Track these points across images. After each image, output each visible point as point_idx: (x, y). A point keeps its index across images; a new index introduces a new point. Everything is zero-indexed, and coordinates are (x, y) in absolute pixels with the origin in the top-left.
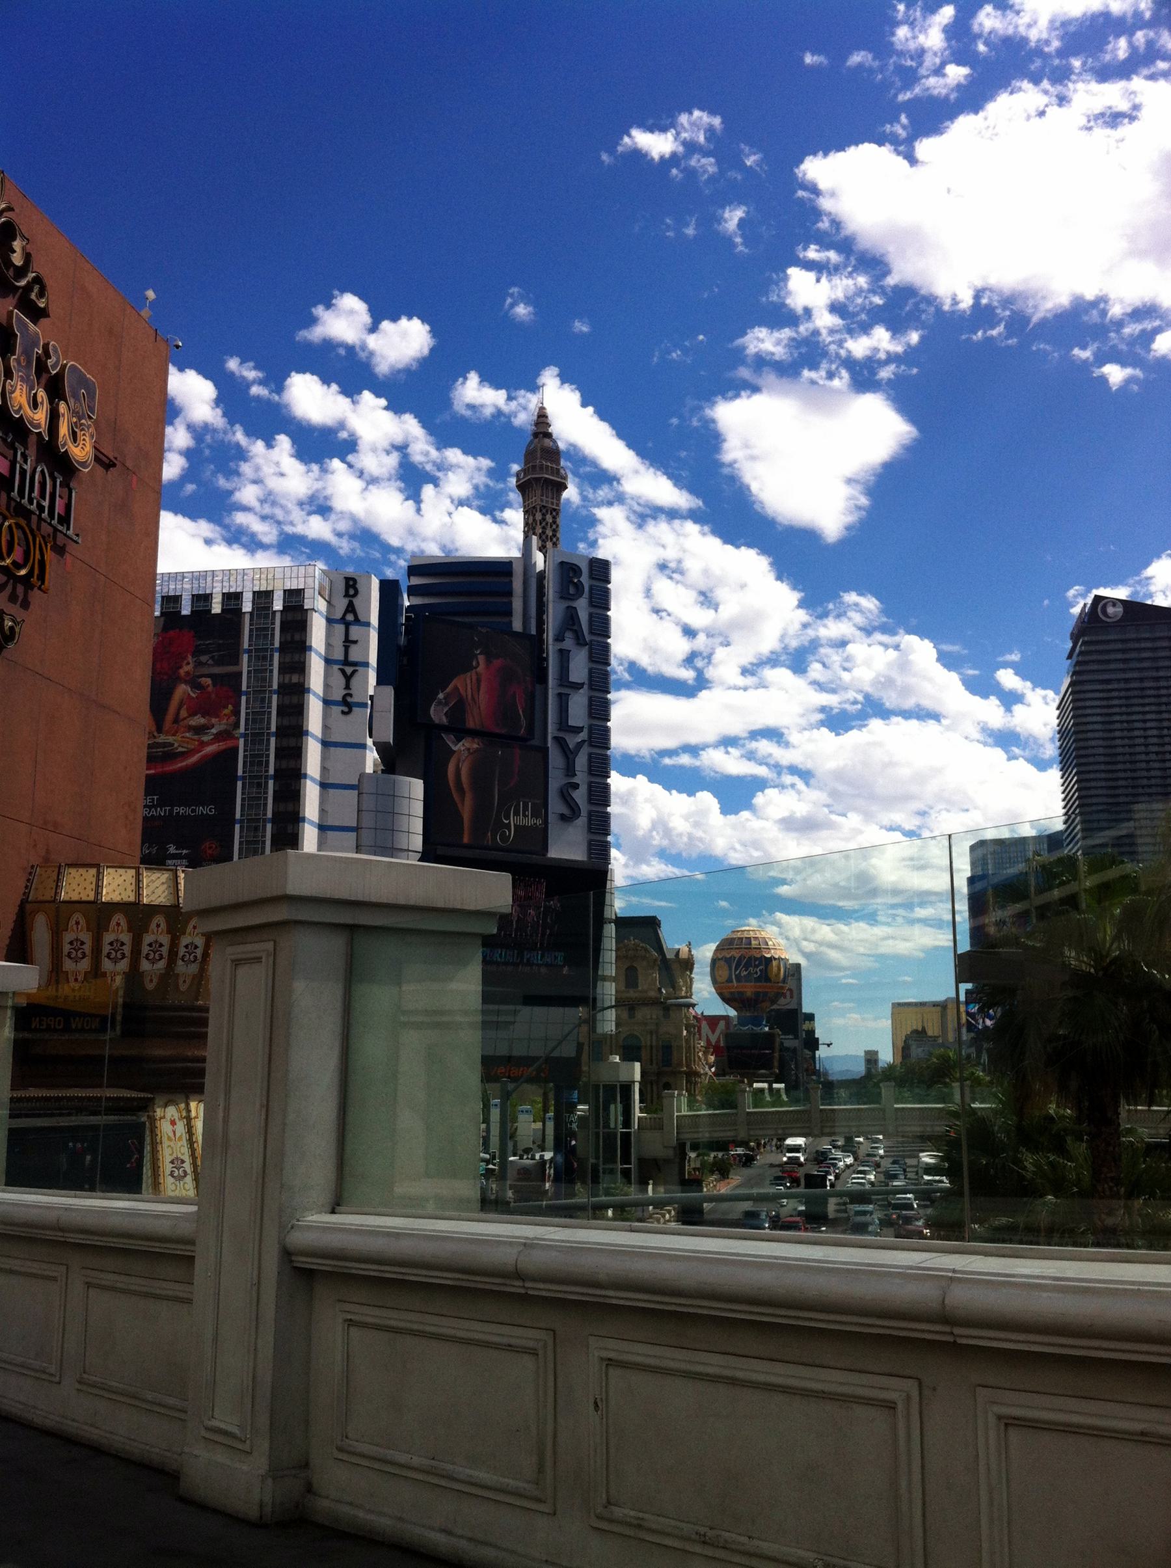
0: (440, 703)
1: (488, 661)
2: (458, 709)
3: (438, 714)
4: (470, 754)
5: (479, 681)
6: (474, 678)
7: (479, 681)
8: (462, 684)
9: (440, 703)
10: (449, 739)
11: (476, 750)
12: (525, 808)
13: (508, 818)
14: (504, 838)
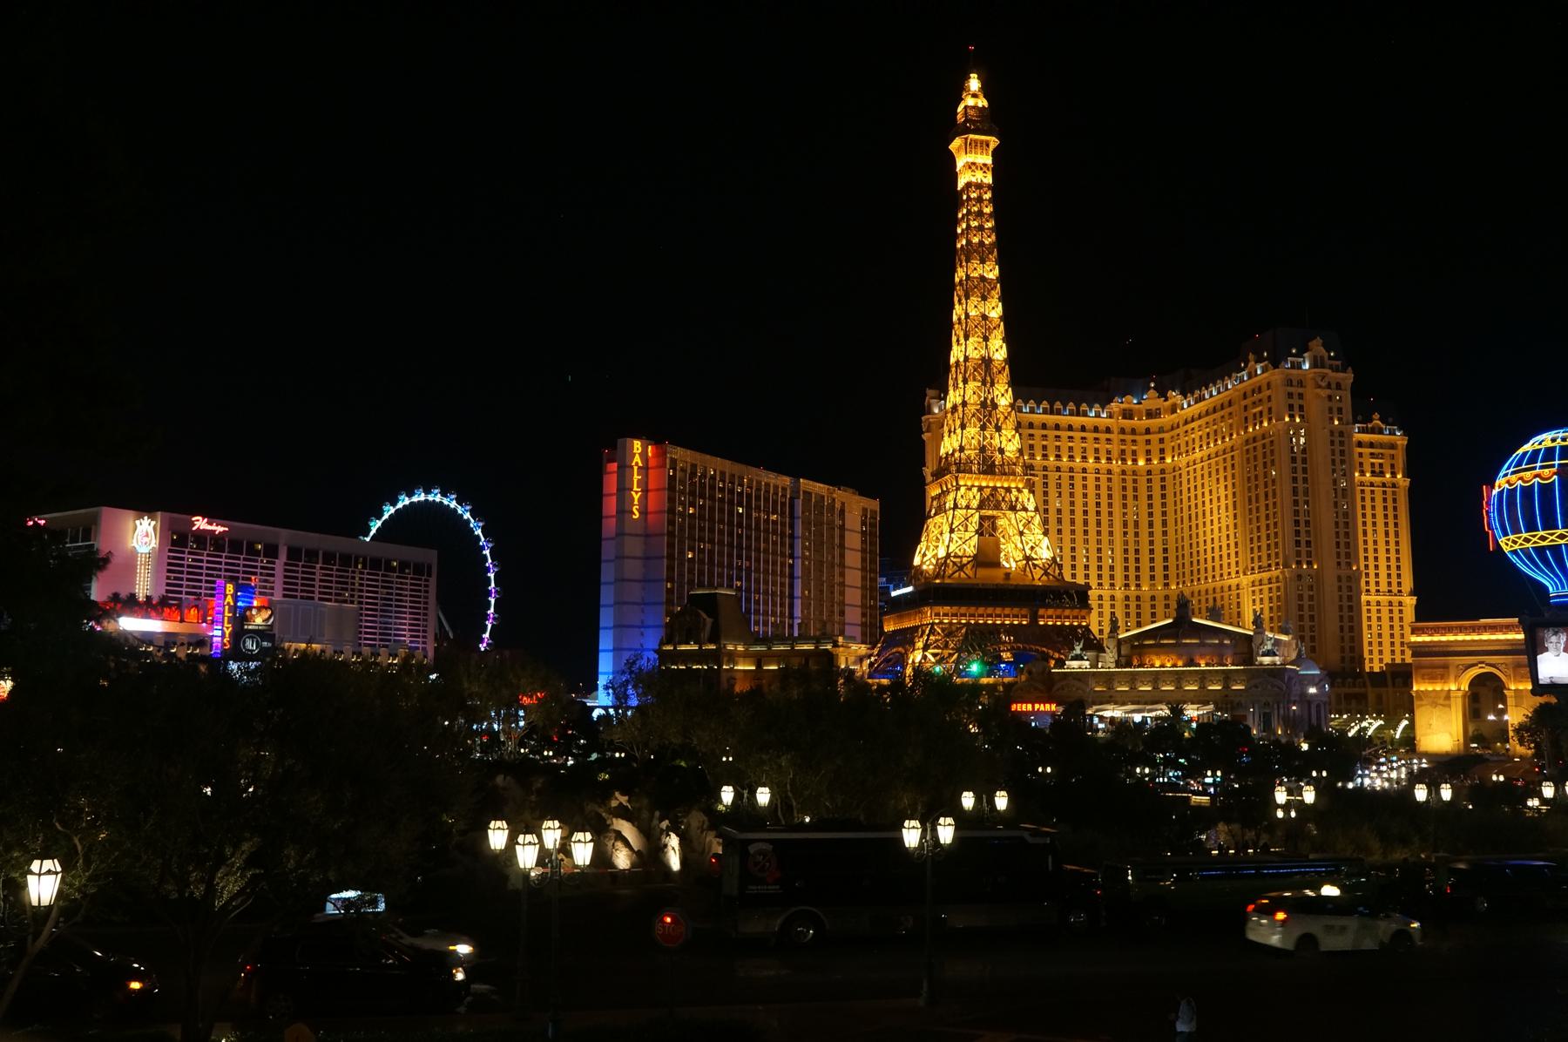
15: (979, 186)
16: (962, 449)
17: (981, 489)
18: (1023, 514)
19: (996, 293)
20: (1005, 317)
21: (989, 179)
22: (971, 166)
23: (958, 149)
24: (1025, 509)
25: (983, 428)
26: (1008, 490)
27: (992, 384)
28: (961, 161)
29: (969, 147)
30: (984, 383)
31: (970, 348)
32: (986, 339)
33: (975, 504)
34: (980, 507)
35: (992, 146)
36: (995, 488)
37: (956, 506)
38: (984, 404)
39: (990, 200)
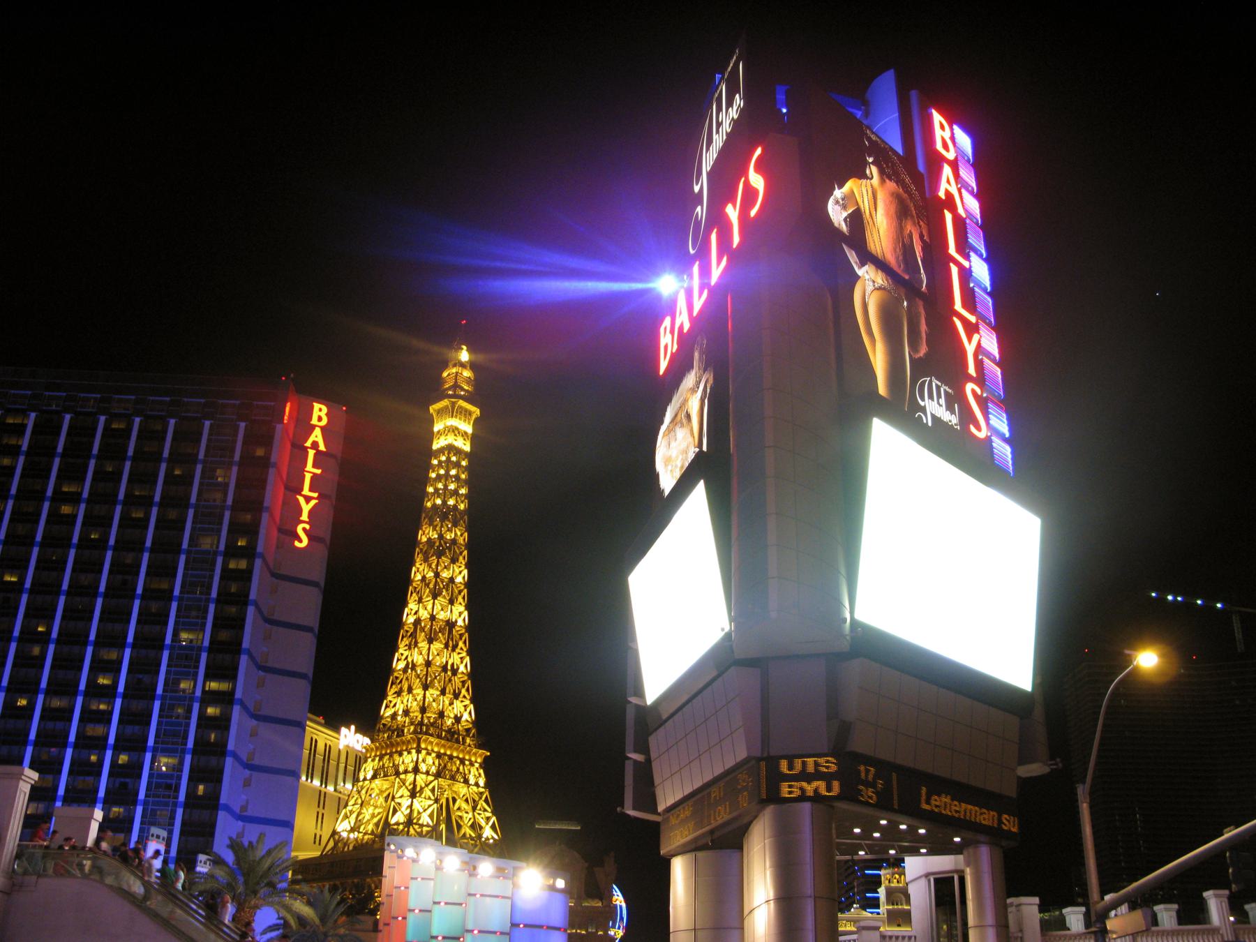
1: (882, 181)
2: (856, 219)
3: (837, 215)
10: (852, 257)
12: (939, 396)
13: (923, 400)
15: (458, 451)
16: (423, 710)
17: (439, 756)
18: (475, 788)
19: (462, 561)
20: (468, 585)
21: (467, 447)
22: (454, 430)
23: (439, 412)
24: (477, 785)
25: (443, 692)
26: (462, 761)
27: (453, 650)
28: (438, 427)
29: (452, 411)
30: (446, 646)
31: (438, 607)
32: (451, 602)
33: (433, 770)
34: (438, 775)
35: (474, 417)
36: (451, 757)
37: (416, 770)
38: (444, 668)
39: (466, 468)
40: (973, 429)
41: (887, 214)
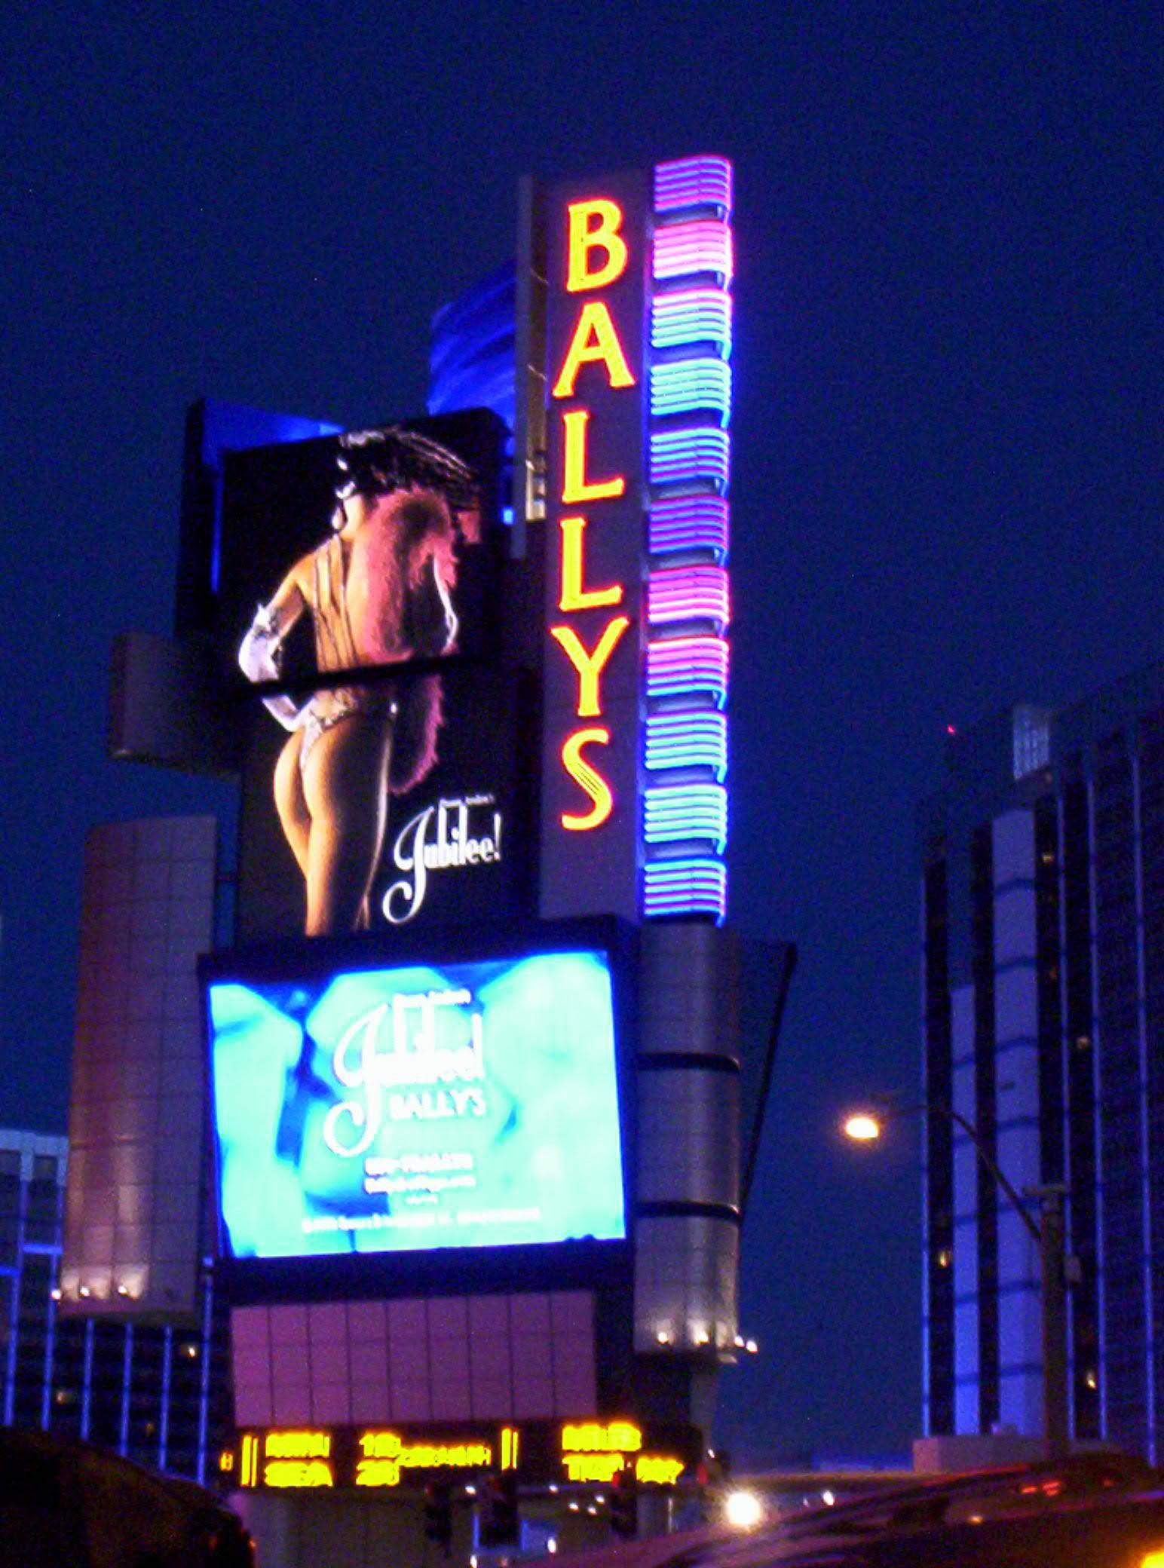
0: (262, 633)
1: (369, 506)
4: (325, 728)
5: (346, 557)
6: (336, 555)
7: (346, 557)
8: (310, 577)
9: (262, 633)
11: (338, 721)
13: (407, 851)
14: (400, 904)
40: (570, 822)
41: (372, 566)
